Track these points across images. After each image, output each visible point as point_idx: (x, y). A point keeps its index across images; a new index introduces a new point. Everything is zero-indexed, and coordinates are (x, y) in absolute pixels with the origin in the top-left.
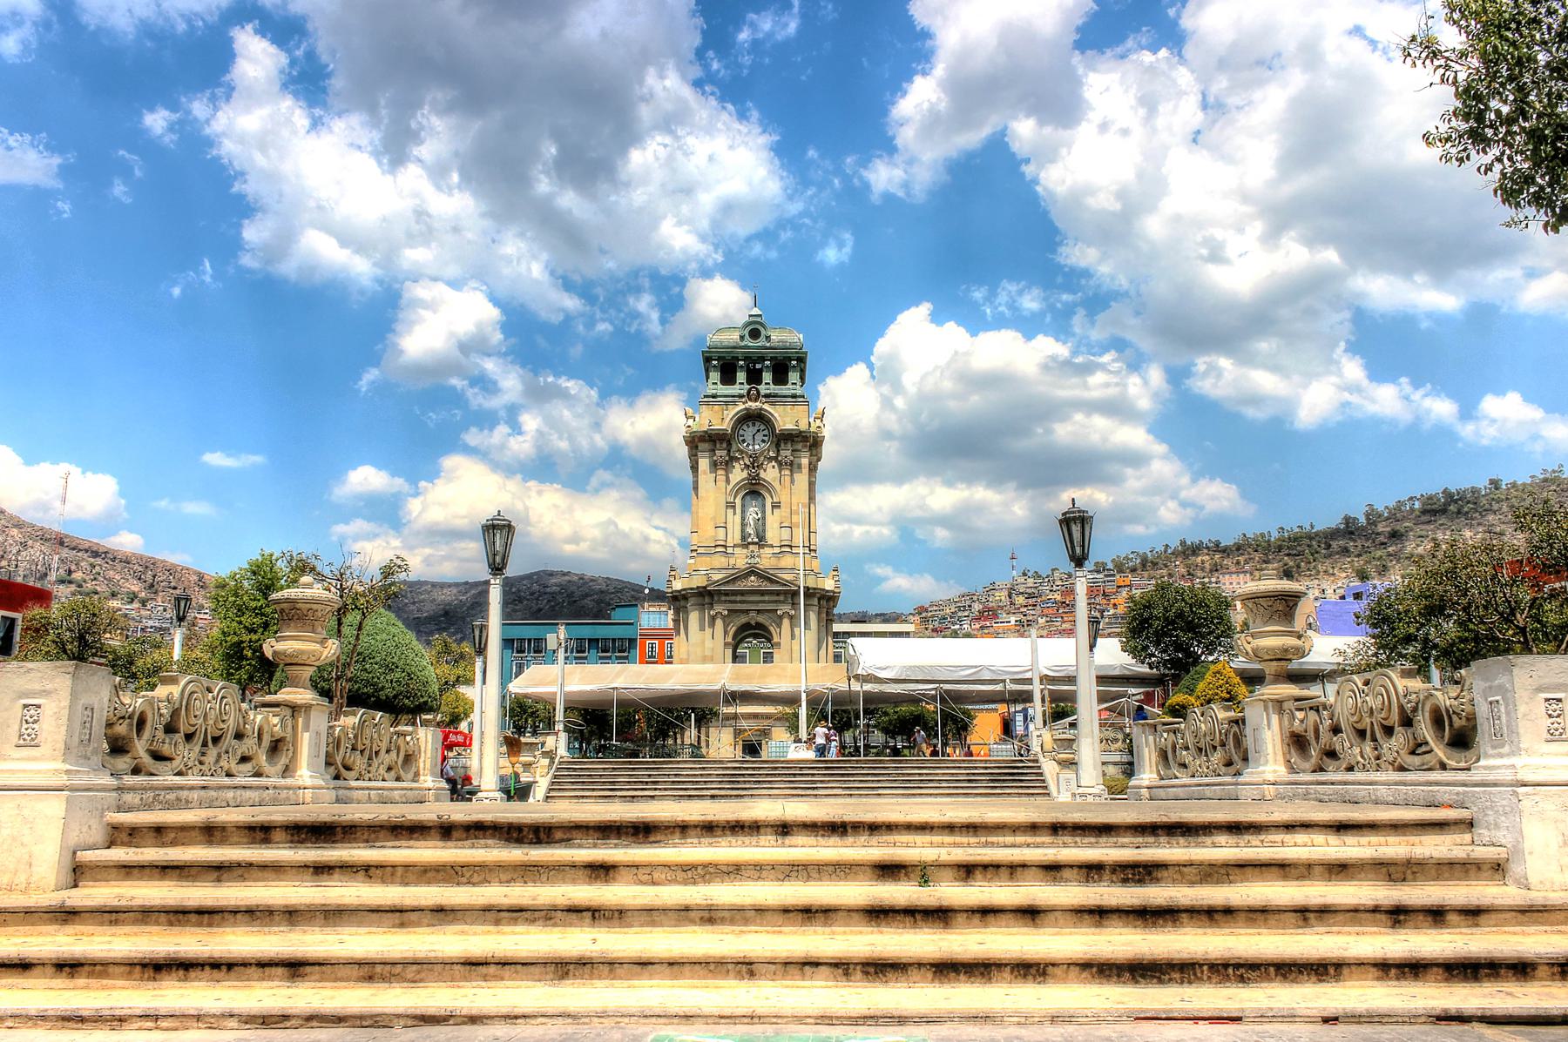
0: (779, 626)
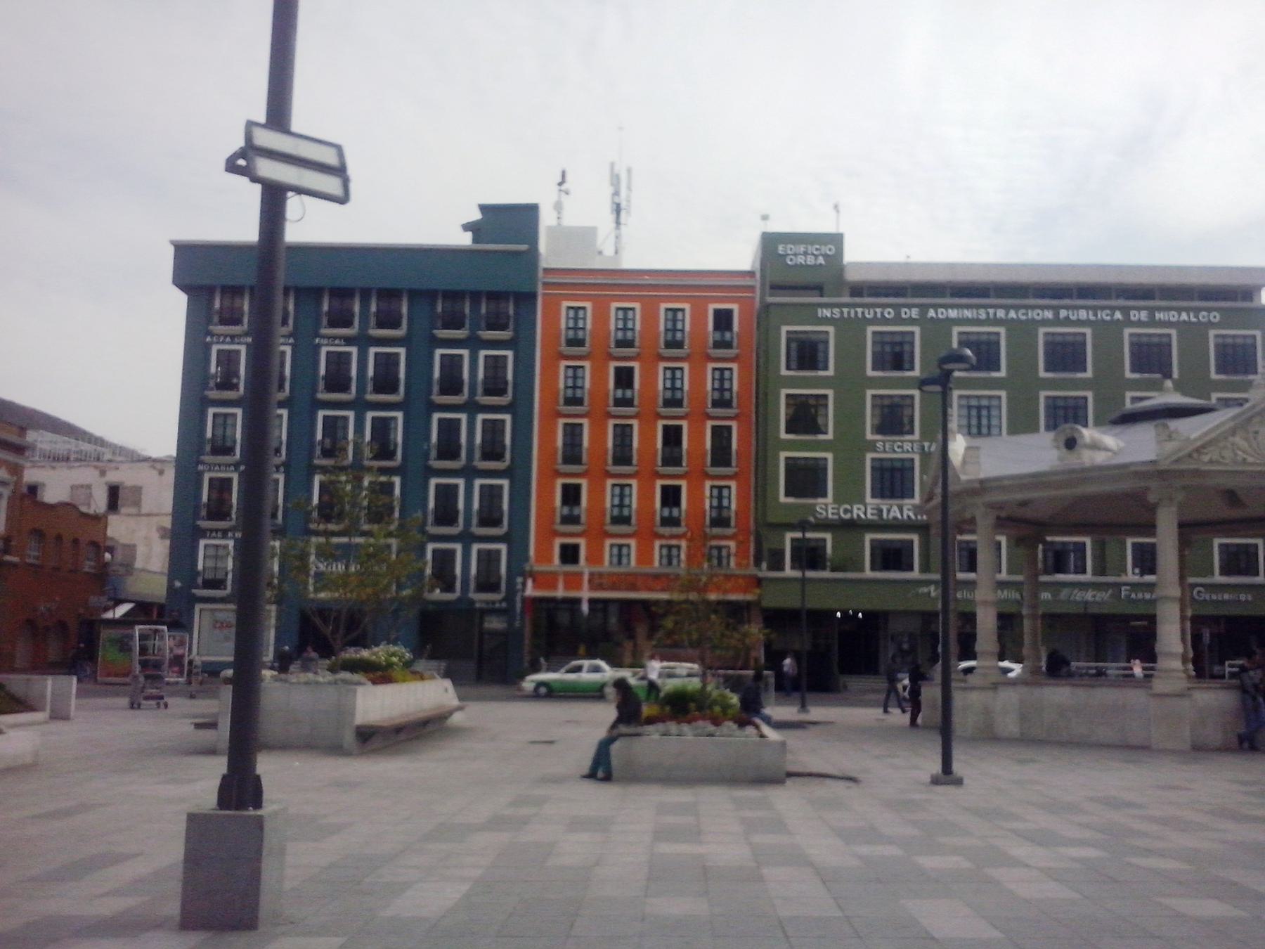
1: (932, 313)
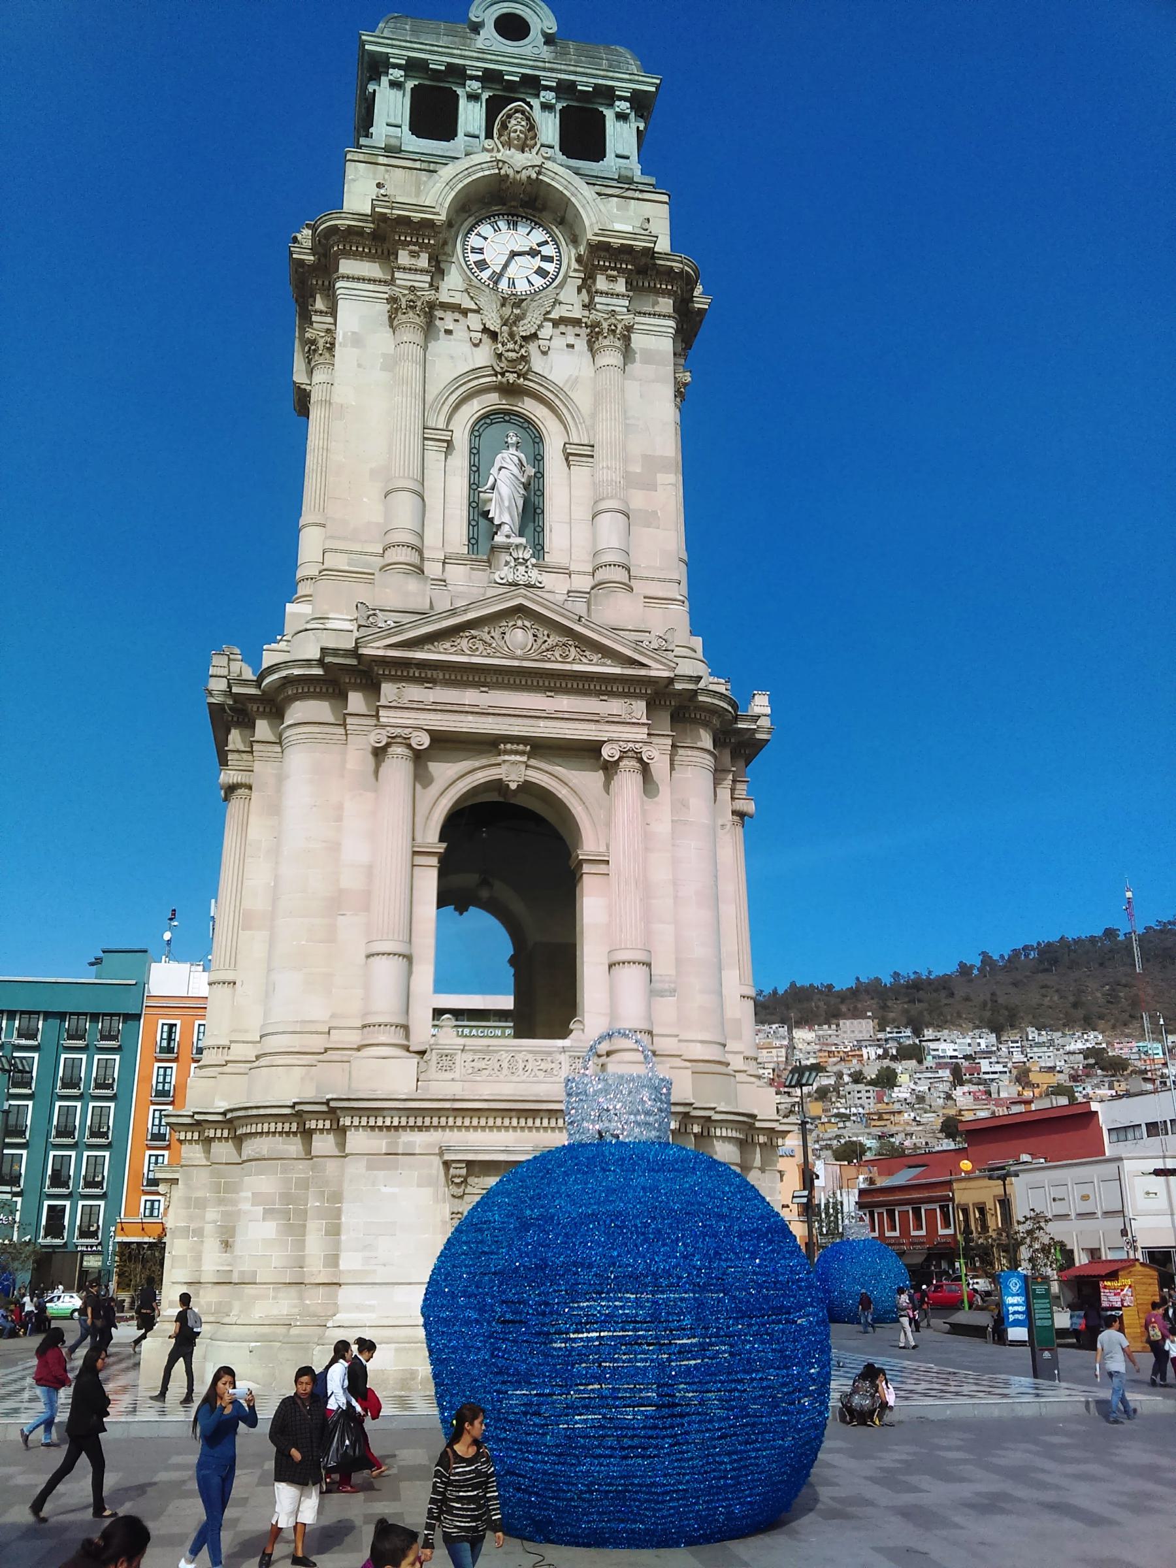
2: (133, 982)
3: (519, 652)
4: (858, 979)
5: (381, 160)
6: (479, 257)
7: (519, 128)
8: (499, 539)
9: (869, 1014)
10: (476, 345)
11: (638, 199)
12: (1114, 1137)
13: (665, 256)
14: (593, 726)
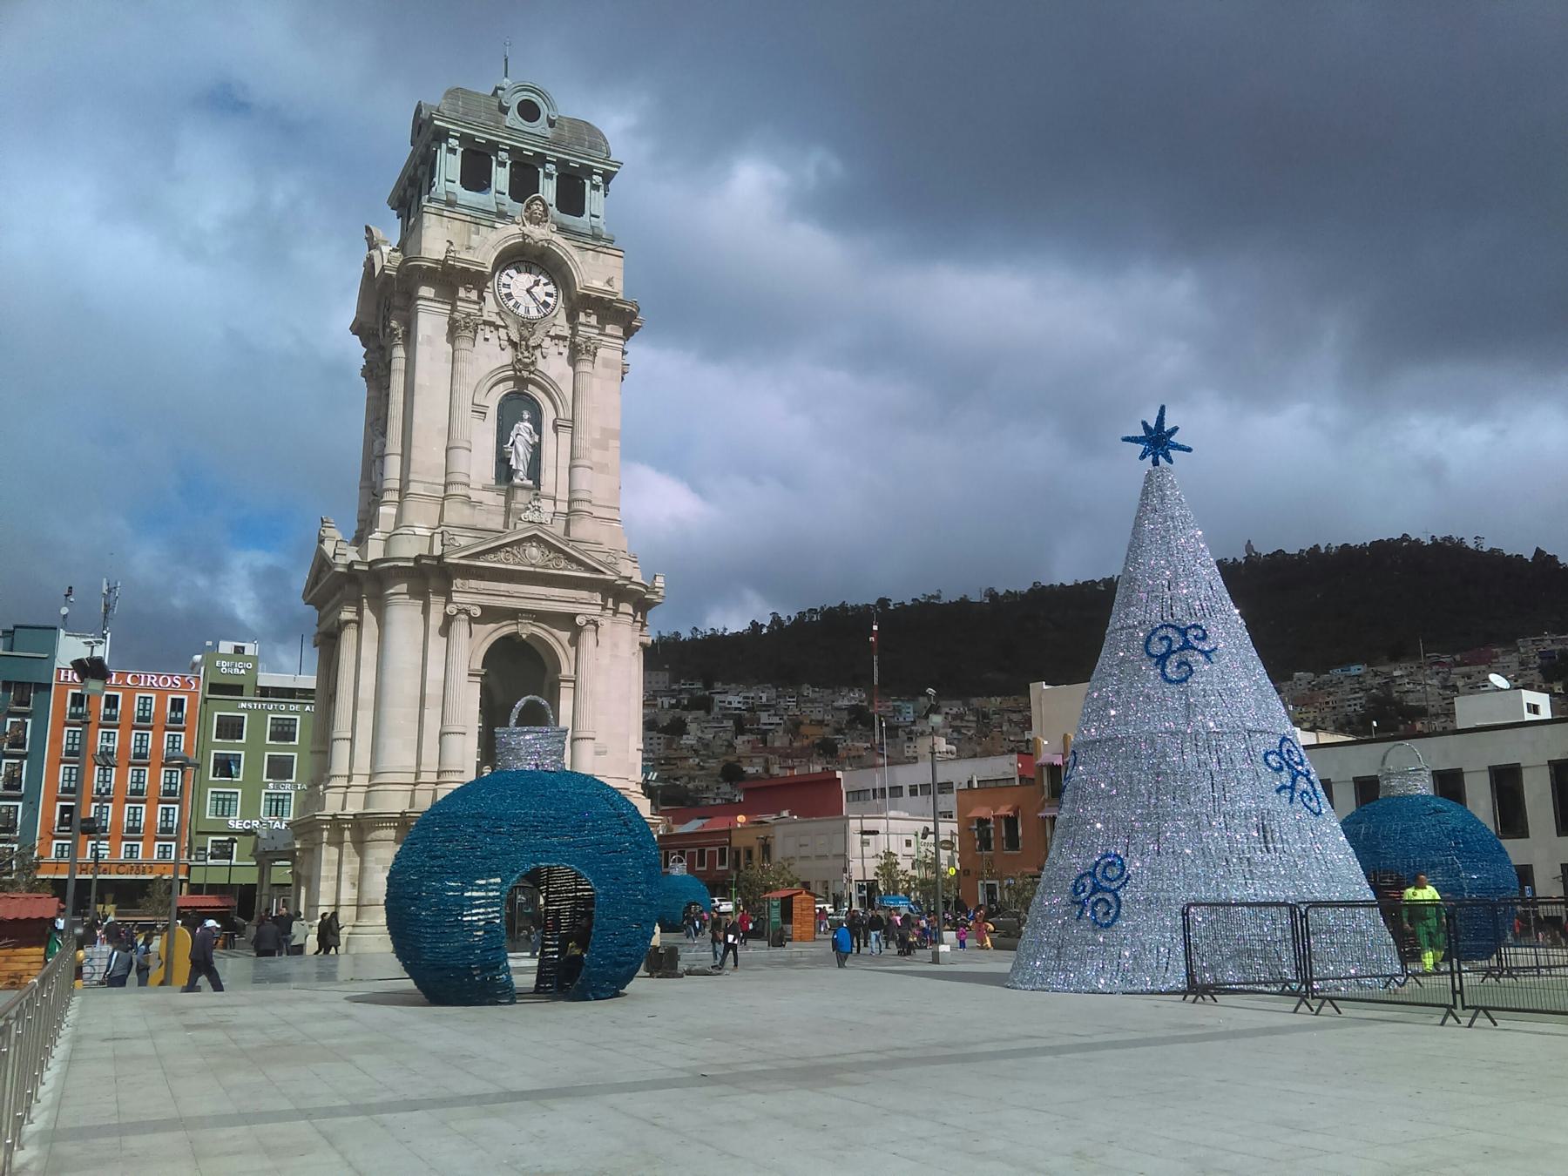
0: (575, 642)
1: (308, 708)
2: (46, 656)
3: (533, 562)
4: (659, 632)
5: (446, 213)
6: (507, 291)
7: (538, 211)
8: (516, 481)
9: (667, 666)
10: (503, 350)
11: (605, 253)
12: (850, 796)
13: (619, 301)
14: (571, 605)
